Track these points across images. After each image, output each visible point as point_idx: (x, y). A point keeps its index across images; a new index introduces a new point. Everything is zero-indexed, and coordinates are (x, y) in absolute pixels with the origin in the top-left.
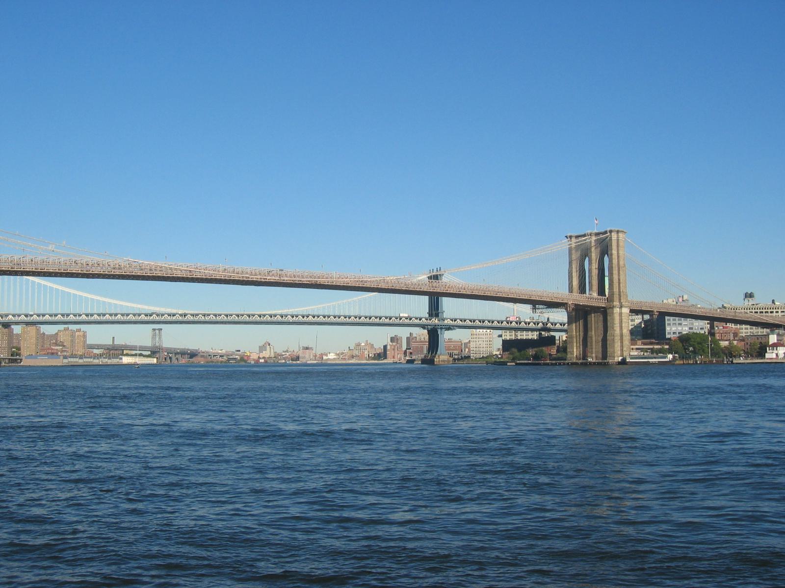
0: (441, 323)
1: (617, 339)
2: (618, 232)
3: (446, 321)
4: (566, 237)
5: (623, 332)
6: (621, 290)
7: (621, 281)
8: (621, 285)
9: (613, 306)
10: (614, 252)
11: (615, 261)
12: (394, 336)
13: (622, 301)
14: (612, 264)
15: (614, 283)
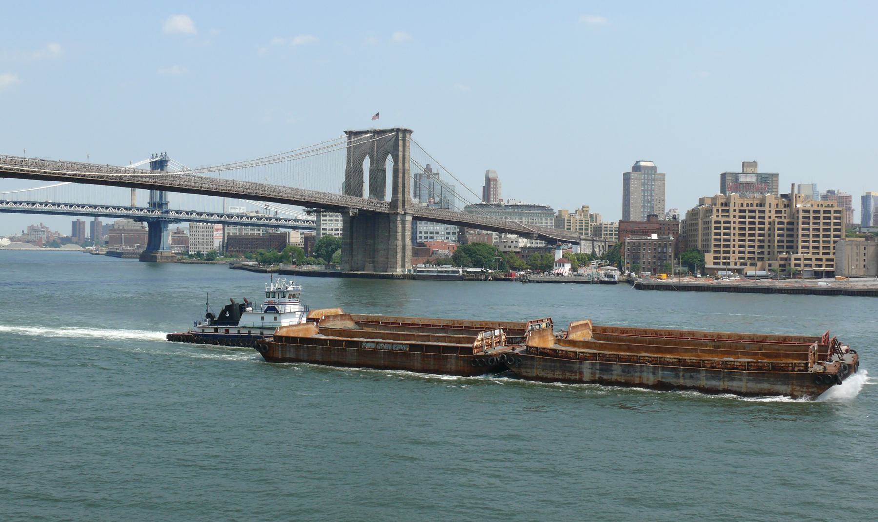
0: (165, 215)
1: (399, 248)
2: (405, 131)
3: (171, 214)
4: (346, 132)
5: (406, 241)
6: (406, 196)
7: (406, 185)
8: (406, 190)
9: (397, 213)
10: (400, 153)
11: (400, 165)
12: (76, 220)
13: (406, 207)
14: (398, 166)
15: (399, 188)
